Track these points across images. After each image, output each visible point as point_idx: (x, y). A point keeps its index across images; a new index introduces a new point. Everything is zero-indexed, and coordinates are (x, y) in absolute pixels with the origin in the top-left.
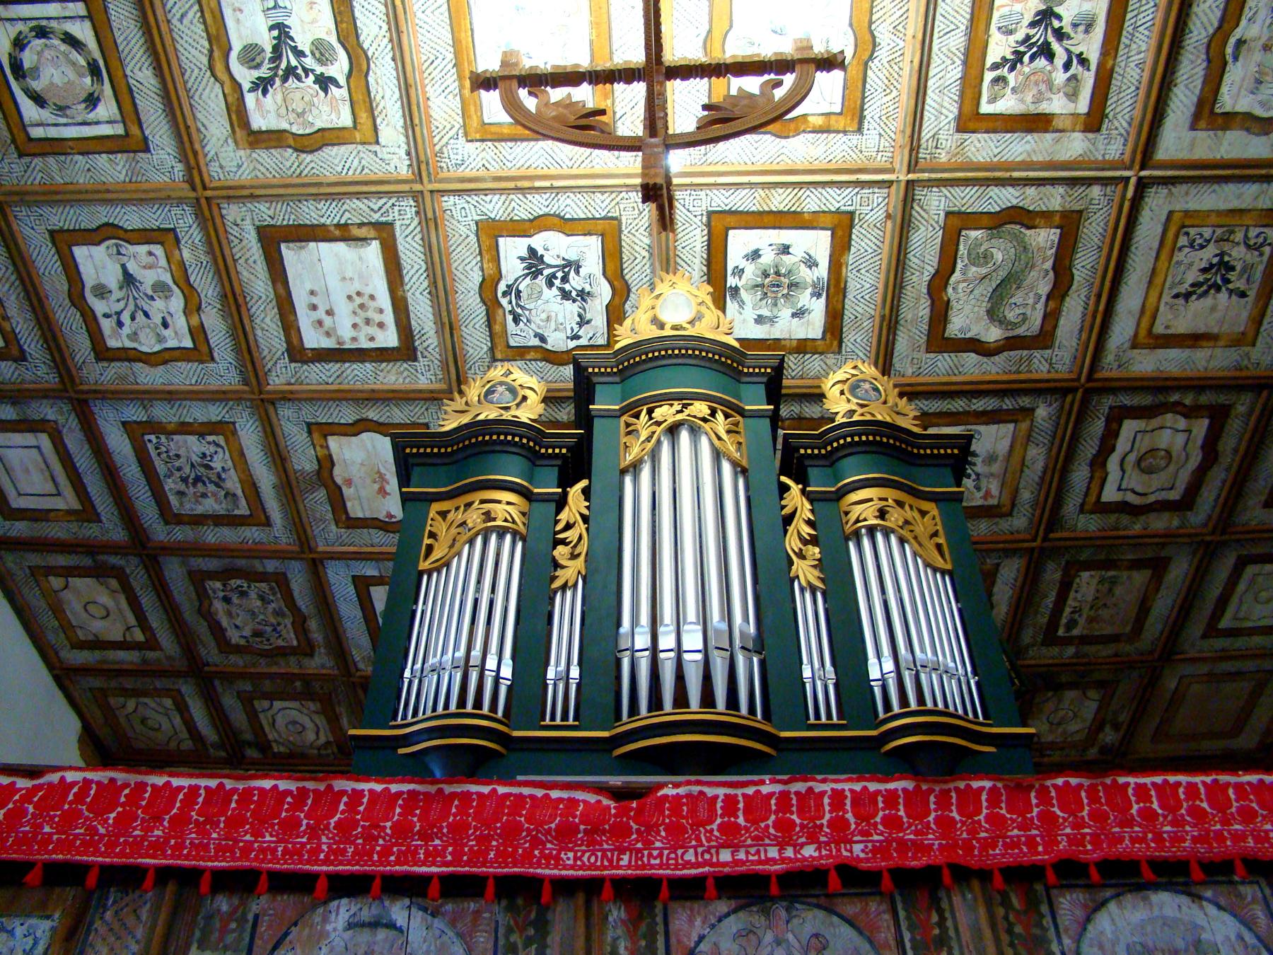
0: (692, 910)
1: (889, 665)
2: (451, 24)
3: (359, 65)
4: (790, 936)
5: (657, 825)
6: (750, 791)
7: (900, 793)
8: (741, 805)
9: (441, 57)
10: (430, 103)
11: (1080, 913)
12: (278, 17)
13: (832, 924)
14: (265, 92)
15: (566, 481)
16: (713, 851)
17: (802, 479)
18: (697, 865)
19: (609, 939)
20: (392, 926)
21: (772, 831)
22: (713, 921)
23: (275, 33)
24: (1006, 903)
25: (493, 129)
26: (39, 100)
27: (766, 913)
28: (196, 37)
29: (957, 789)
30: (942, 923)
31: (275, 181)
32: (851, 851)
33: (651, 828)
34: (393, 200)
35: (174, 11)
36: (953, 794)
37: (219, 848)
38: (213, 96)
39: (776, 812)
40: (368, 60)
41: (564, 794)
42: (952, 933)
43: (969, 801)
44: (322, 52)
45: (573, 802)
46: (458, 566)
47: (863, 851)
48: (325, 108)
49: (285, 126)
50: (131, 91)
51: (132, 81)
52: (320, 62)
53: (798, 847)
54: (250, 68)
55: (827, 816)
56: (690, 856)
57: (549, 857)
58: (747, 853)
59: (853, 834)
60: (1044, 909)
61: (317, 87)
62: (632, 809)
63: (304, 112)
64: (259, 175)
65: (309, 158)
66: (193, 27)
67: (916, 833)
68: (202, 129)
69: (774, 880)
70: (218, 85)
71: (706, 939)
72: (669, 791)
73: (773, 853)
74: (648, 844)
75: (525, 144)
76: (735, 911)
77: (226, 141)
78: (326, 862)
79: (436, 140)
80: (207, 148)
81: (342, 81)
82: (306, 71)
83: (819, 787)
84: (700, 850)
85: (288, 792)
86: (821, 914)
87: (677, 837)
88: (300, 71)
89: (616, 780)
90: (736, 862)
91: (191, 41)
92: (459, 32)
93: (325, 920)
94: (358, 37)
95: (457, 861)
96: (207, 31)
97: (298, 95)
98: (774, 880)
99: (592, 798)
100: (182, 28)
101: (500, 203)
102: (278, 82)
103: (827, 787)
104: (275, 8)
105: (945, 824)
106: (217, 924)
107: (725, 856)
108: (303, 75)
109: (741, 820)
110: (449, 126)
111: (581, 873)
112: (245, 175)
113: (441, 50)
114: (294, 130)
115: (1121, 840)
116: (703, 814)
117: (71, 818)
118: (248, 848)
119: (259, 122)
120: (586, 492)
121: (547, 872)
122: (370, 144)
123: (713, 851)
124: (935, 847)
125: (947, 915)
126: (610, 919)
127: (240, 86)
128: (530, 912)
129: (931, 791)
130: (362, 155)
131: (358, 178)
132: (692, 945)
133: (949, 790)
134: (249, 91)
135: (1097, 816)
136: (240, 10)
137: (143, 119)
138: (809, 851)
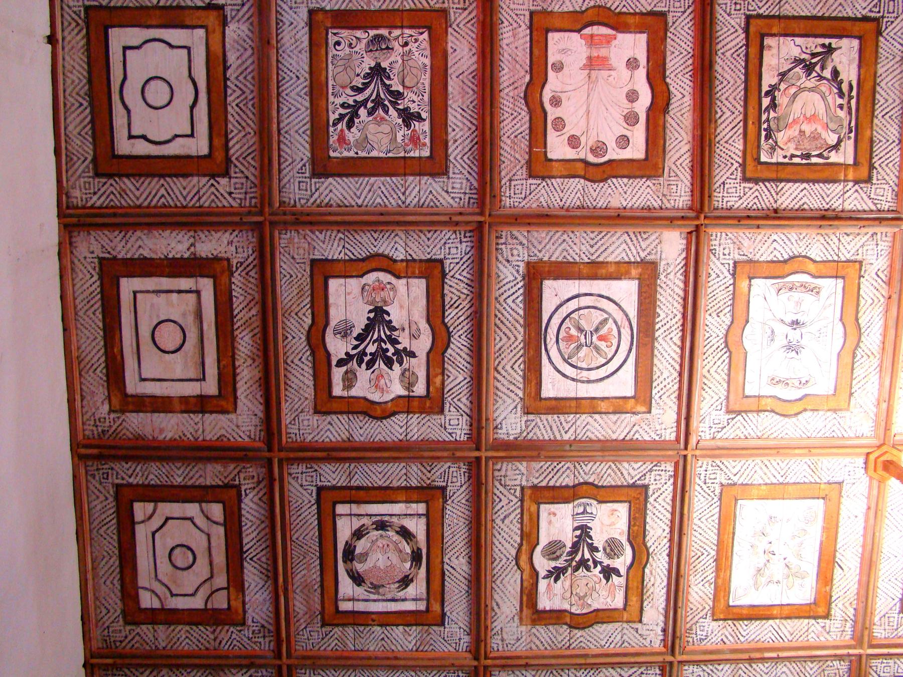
2: (719, 530)
9: (706, 553)
10: (690, 590)
12: (583, 520)
14: (556, 580)
23: (578, 532)
25: (735, 610)
26: (358, 579)
28: (512, 534)
31: (547, 653)
34: (642, 670)
35: (499, 513)
38: (512, 581)
40: (648, 554)
44: (613, 548)
48: (604, 593)
49: (566, 606)
50: (443, 574)
51: (446, 566)
52: (609, 556)
54: (550, 559)
61: (601, 576)
63: (586, 595)
64: (534, 647)
65: (579, 633)
66: (511, 526)
68: (496, 608)
70: (519, 572)
75: (758, 622)
77: (513, 618)
79: (688, 619)
80: (495, 624)
81: (623, 571)
82: (596, 563)
88: (590, 563)
91: (506, 536)
92: (724, 534)
94: (644, 536)
97: (584, 582)
100: (502, 526)
101: (729, 671)
104: (582, 513)
108: (592, 566)
110: (701, 608)
112: (521, 648)
113: (707, 548)
114: (574, 610)
119: (544, 603)
122: (634, 622)
127: (537, 574)
130: (625, 631)
131: (620, 651)
134: (544, 578)
136: (555, 514)
137: (447, 597)
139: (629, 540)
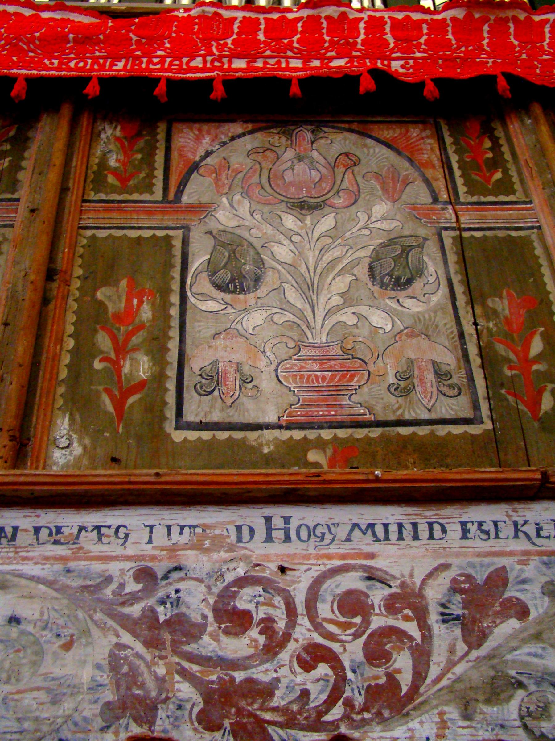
0: (200, 130)
4: (315, 154)
5: (162, 38)
7: (449, 22)
8: (262, 27)
13: (365, 145)
16: (225, 60)
18: (204, 70)
19: (99, 153)
21: (296, 45)
22: (224, 139)
27: (289, 135)
29: (515, 19)
32: (389, 65)
36: (511, 25)
39: (301, 32)
42: (507, 156)
47: (402, 67)
55: (362, 36)
58: (265, 63)
59: (392, 51)
62: (135, 24)
69: (295, 83)
71: (214, 155)
73: (296, 63)
74: (149, 55)
76: (251, 132)
84: (209, 58)
98: (295, 83)
107: (240, 64)
111: (63, 73)
121: (24, 72)
123: (225, 60)
124: (490, 64)
125: (502, 141)
126: (103, 136)
128: (9, 131)
129: (485, 20)
132: (197, 159)
133: (507, 20)
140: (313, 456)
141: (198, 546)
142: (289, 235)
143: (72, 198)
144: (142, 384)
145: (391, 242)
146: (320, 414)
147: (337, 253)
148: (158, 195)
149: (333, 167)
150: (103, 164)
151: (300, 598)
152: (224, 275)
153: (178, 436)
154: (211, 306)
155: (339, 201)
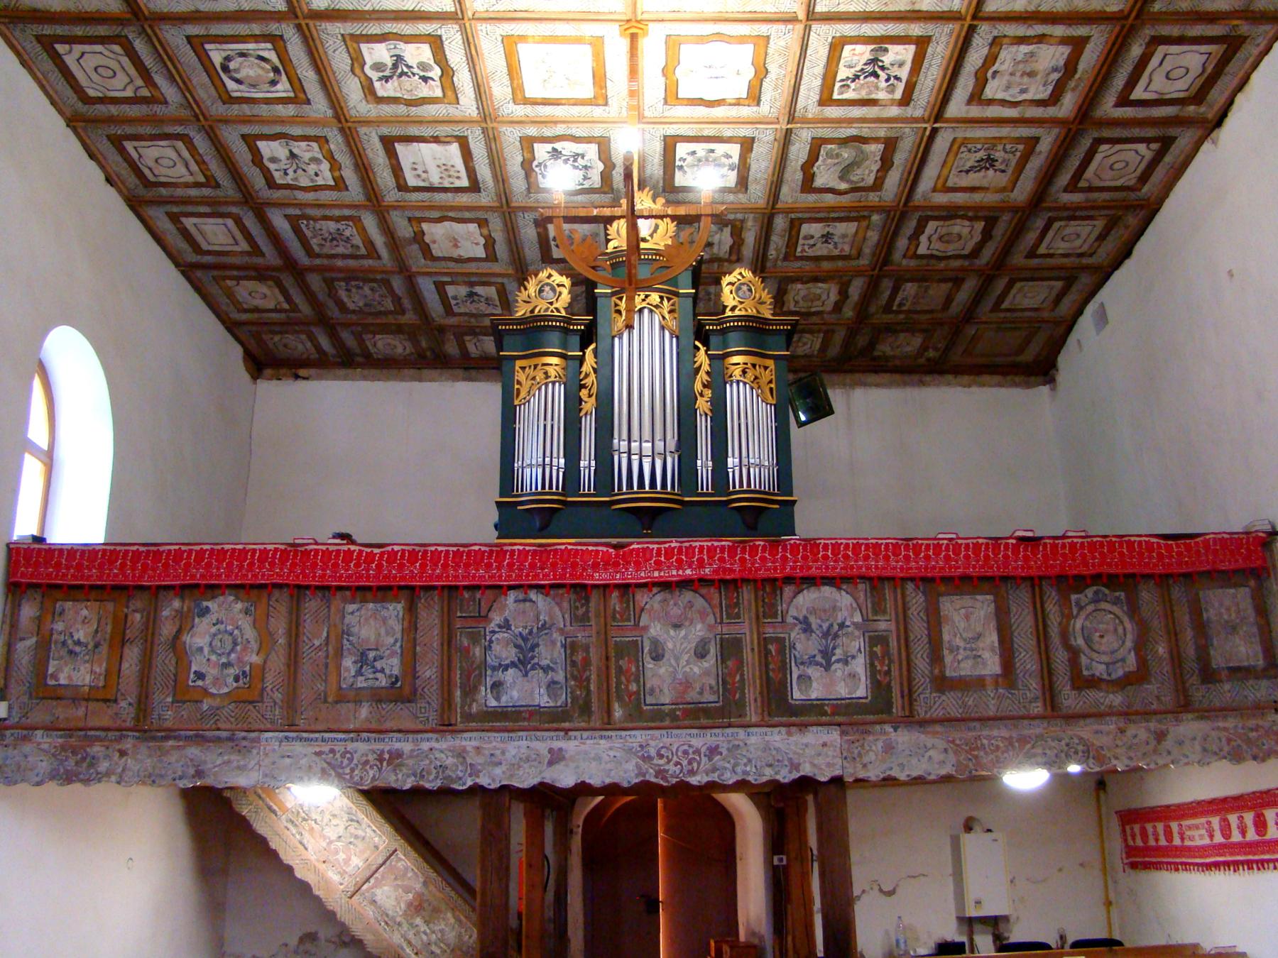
1: (737, 460)
3: (448, 74)
6: (667, 545)
11: (791, 594)
12: (397, 52)
14: (387, 81)
15: (583, 348)
17: (706, 344)
20: (531, 601)
24: (764, 589)
26: (239, 81)
27: (671, 592)
30: (738, 598)
33: (628, 563)
37: (463, 577)
41: (594, 548)
43: (754, 550)
45: (597, 551)
46: (534, 402)
50: (300, 80)
53: (684, 570)
56: (643, 574)
57: (589, 576)
60: (778, 592)
67: (731, 564)
72: (635, 546)
73: (674, 572)
74: (627, 569)
78: (505, 581)
82: (414, 74)
83: (694, 544)
85: (485, 551)
86: (691, 593)
87: (638, 566)
89: (614, 541)
90: (661, 577)
93: (506, 600)
95: (555, 579)
96: (350, 56)
99: (605, 549)
102: (395, 78)
103: (697, 544)
105: (743, 560)
106: (465, 603)
107: (656, 574)
109: (663, 559)
115: (810, 568)
116: (648, 556)
117: (401, 566)
118: (474, 576)
120: (595, 352)
127: (371, 79)
135: (805, 558)
138: (688, 572)
139: (435, 62)
140: (678, 713)
141: (652, 739)
142: (672, 638)
143: (609, 627)
144: (635, 693)
145: (702, 640)
146: (679, 700)
147: (685, 645)
148: (632, 623)
149: (685, 608)
150: (615, 609)
151: (674, 750)
152: (654, 655)
153: (645, 708)
154: (650, 666)
155: (687, 623)
